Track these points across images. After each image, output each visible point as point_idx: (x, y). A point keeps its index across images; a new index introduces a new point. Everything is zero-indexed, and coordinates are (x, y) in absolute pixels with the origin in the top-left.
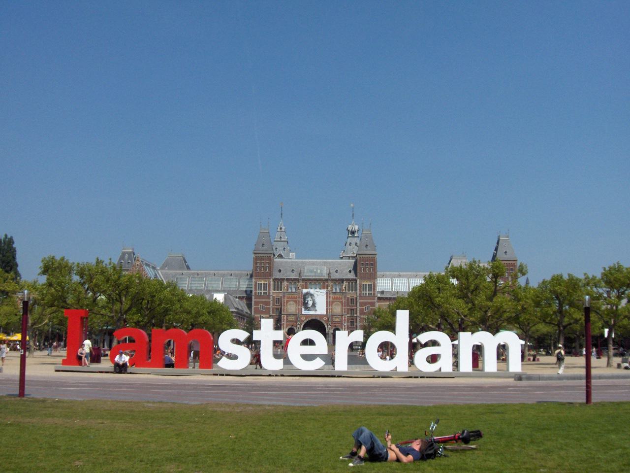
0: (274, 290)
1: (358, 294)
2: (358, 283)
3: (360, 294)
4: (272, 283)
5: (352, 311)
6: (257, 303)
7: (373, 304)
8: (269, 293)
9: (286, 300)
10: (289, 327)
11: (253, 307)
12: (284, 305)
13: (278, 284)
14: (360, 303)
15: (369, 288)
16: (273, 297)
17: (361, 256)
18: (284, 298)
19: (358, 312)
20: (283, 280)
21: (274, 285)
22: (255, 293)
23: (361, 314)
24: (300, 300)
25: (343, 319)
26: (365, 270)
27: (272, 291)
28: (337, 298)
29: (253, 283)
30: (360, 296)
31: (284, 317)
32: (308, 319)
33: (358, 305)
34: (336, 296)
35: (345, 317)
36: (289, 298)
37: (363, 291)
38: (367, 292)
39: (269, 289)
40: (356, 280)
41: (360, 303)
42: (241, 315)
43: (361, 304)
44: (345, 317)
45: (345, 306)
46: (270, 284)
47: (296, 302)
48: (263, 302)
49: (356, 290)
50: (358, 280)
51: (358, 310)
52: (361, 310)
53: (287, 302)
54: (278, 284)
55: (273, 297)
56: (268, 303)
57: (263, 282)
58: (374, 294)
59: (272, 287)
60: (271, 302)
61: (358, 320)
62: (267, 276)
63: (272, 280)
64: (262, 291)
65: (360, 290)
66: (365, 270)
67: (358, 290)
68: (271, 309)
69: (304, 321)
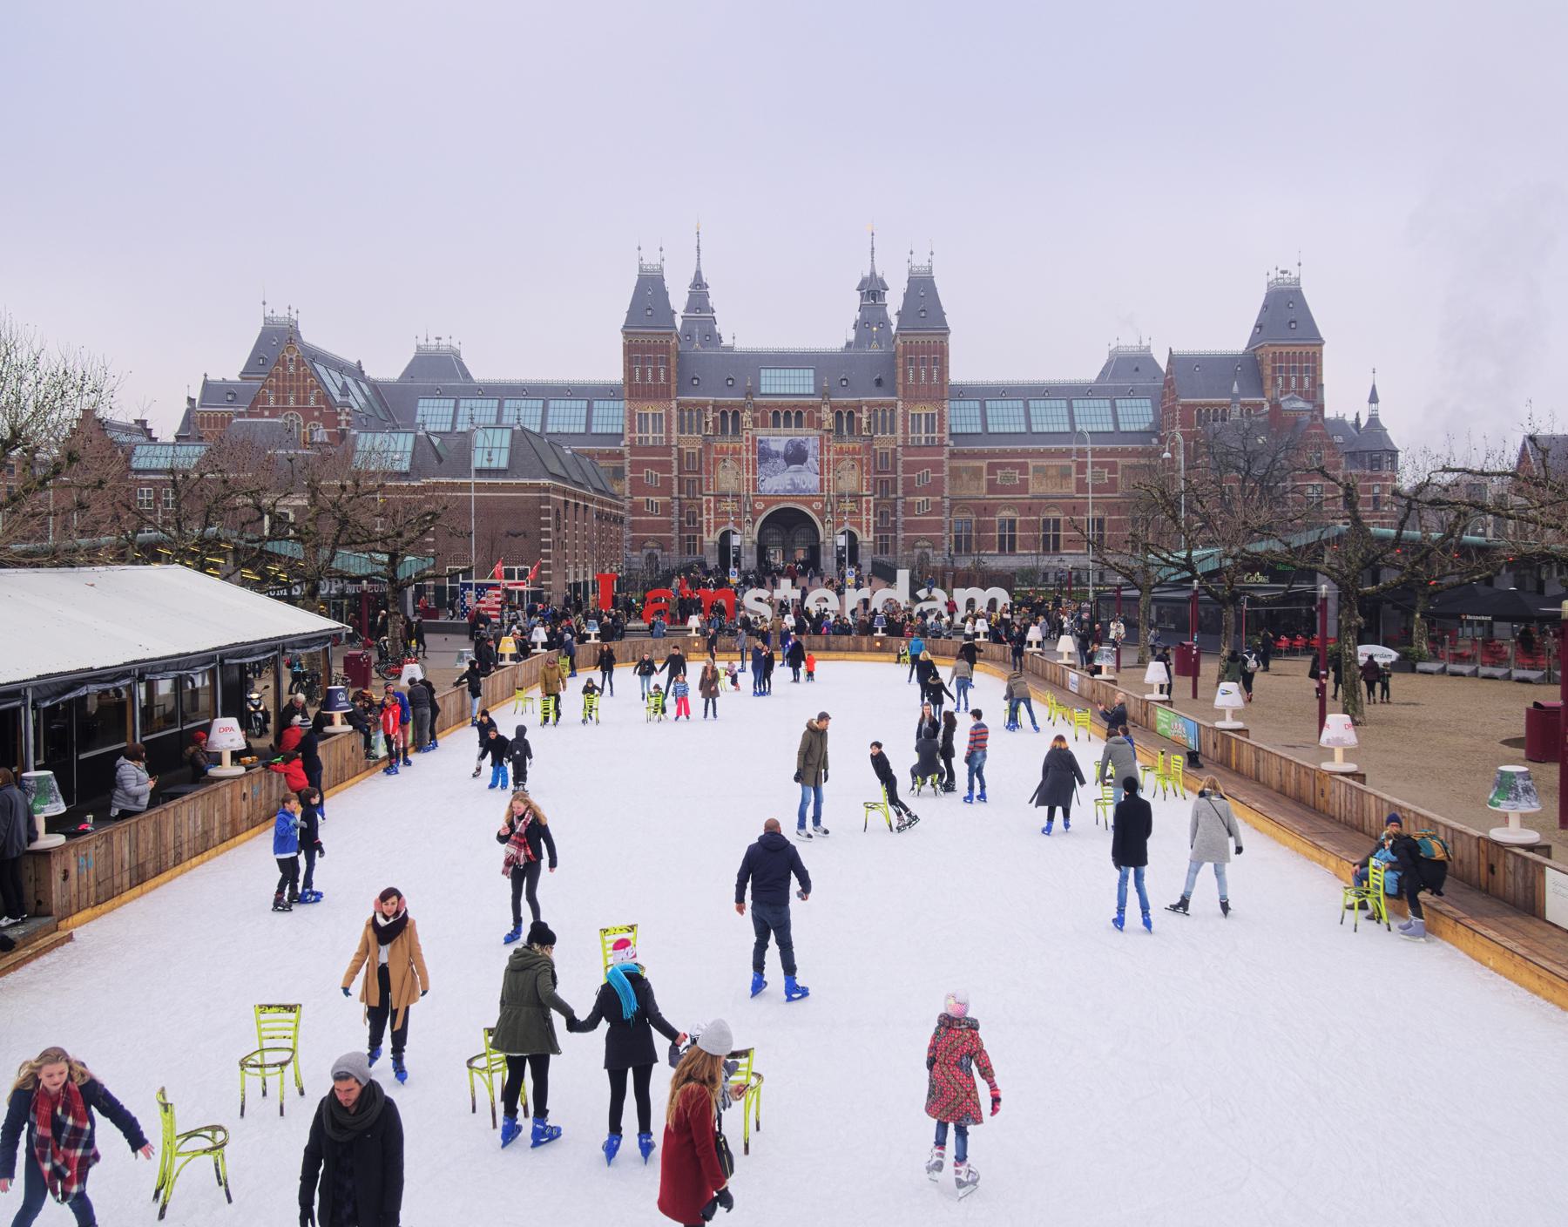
0: (682, 431)
1: (900, 442)
2: (900, 411)
3: (905, 439)
4: (675, 412)
5: (883, 487)
6: (636, 466)
7: (937, 467)
8: (669, 439)
9: (713, 455)
10: (722, 529)
11: (628, 475)
12: (708, 472)
13: (691, 416)
14: (906, 463)
16: (680, 451)
17: (908, 339)
18: (708, 453)
19: (900, 486)
20: (705, 406)
21: (681, 418)
22: (632, 439)
23: (906, 494)
27: (675, 434)
30: (905, 446)
31: (708, 501)
32: (774, 508)
33: (900, 469)
34: (845, 446)
35: (868, 502)
36: (722, 451)
38: (923, 435)
39: (669, 430)
40: (893, 406)
41: (906, 463)
42: (575, 495)
43: (909, 467)
44: (868, 502)
45: (868, 472)
46: (669, 416)
47: (739, 461)
48: (652, 464)
49: (893, 431)
51: (900, 483)
52: (908, 484)
54: (691, 416)
55: (680, 451)
56: (665, 467)
57: (650, 411)
58: (941, 439)
59: (674, 426)
60: (675, 464)
61: (899, 508)
62: (661, 394)
63: (674, 404)
64: (651, 435)
65: (905, 431)
68: (675, 482)
69: (761, 512)
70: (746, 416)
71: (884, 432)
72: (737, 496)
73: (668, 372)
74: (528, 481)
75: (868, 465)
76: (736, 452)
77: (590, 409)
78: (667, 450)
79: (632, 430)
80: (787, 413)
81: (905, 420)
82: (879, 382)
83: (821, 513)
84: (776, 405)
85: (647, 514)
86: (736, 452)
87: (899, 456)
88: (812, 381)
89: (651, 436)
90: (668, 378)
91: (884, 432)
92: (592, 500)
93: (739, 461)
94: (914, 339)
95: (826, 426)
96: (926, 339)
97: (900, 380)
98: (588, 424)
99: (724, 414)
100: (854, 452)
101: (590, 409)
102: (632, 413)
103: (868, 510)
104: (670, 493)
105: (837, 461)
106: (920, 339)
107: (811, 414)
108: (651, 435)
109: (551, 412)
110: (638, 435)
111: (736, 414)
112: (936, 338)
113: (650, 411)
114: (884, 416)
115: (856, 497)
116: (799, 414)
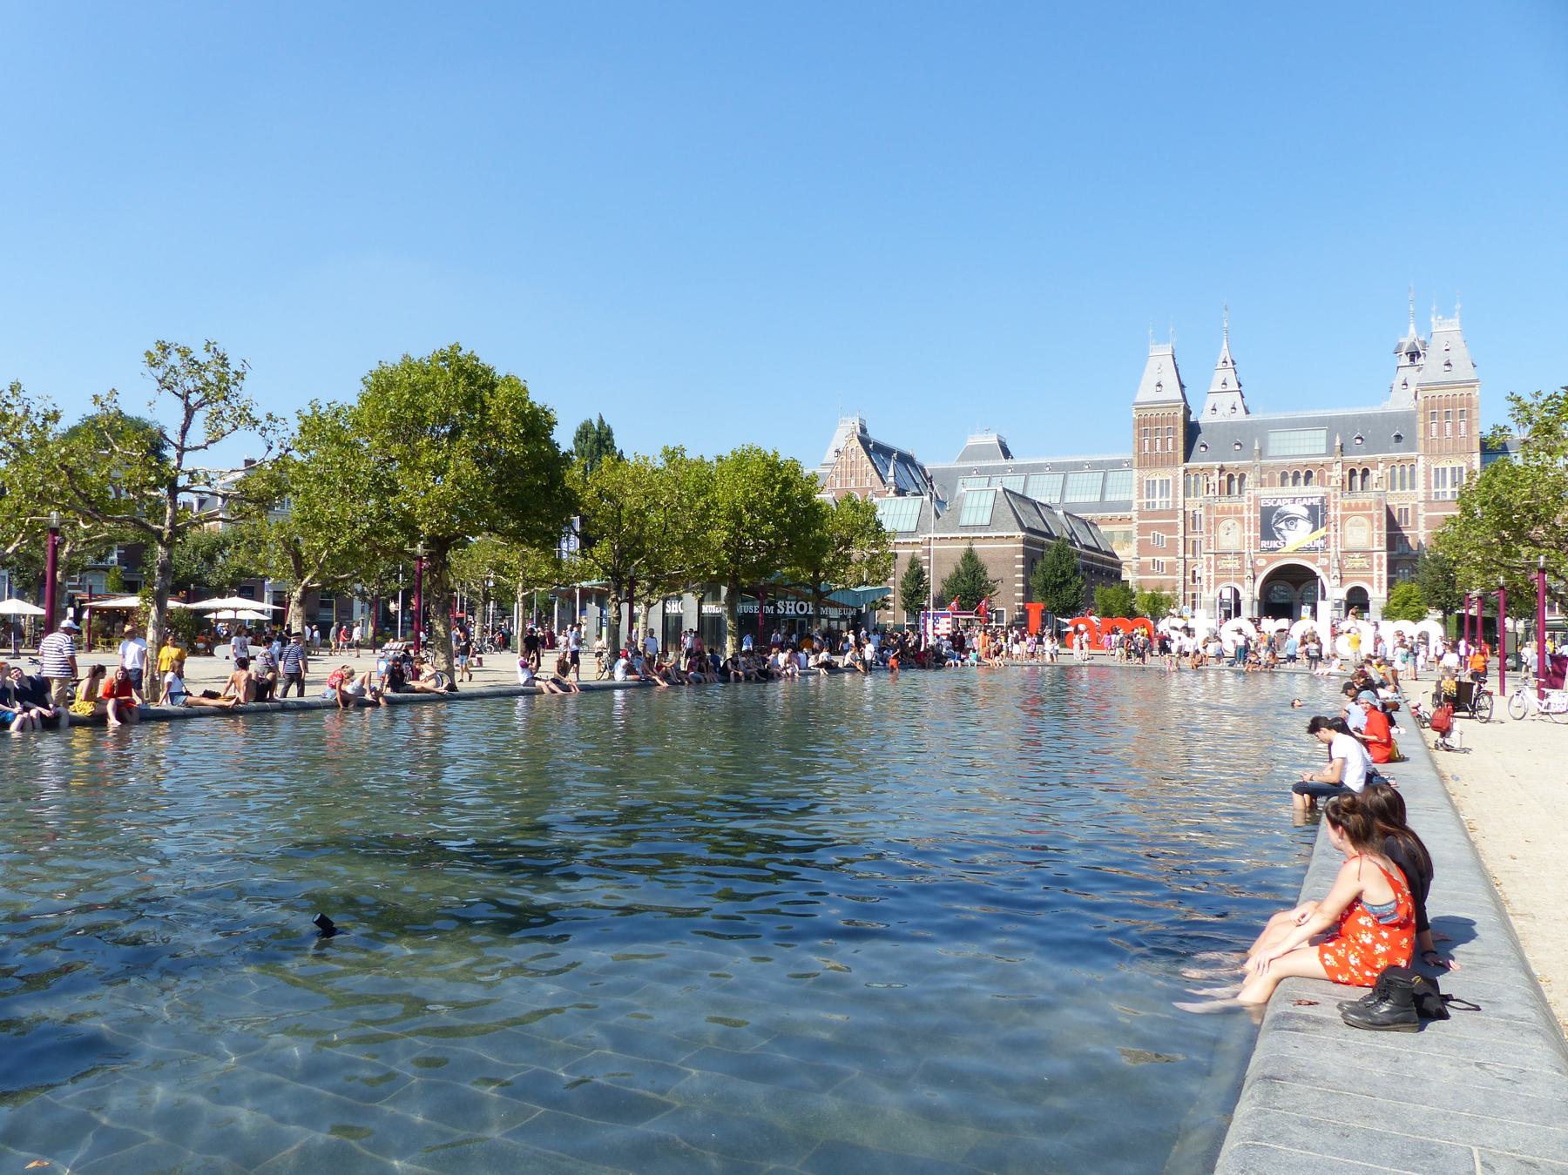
0: (1186, 494)
2: (1420, 467)
3: (1428, 495)
6: (1143, 529)
8: (1175, 503)
12: (1209, 531)
15: (1453, 477)
20: (1212, 469)
22: (1140, 505)
24: (1252, 515)
25: (1376, 561)
26: (1441, 430)
28: (1357, 508)
29: (1135, 482)
30: (1428, 501)
34: (1353, 502)
35: (1380, 558)
36: (1223, 511)
37: (1437, 486)
39: (1175, 495)
44: (1380, 558)
46: (1176, 482)
47: (1242, 520)
49: (1413, 486)
50: (1421, 459)
53: (1217, 521)
56: (1172, 529)
57: (1158, 478)
63: (1181, 470)
64: (1157, 500)
65: (1428, 487)
66: (1441, 430)
67: (1420, 489)
68: (1181, 543)
70: (1250, 479)
71: (1403, 487)
72: (1240, 554)
73: (1175, 441)
74: (1005, 534)
75: (1380, 520)
76: (1238, 511)
77: (1105, 479)
78: (1173, 513)
79: (1140, 496)
80: (1296, 475)
81: (1427, 474)
82: (1398, 437)
83: (1326, 569)
84: (1284, 465)
85: (1152, 573)
86: (1238, 511)
87: (1420, 511)
88: (1324, 442)
89: (1159, 501)
90: (1175, 447)
91: (1403, 487)
92: (1079, 554)
93: (1242, 520)
94: (1437, 393)
95: (1333, 483)
96: (1451, 392)
97: (1421, 434)
98: (1103, 494)
99: (1231, 477)
100: (1364, 507)
101: (1105, 479)
102: (1140, 481)
103: (1380, 565)
104: (1175, 554)
105: (1344, 518)
106: (1444, 393)
107: (1321, 476)
108: (1157, 500)
109: (1069, 484)
110: (1145, 500)
111: (1242, 477)
112: (1465, 391)
113: (1158, 478)
114: (1403, 472)
115: (1367, 553)
116: (1309, 475)
